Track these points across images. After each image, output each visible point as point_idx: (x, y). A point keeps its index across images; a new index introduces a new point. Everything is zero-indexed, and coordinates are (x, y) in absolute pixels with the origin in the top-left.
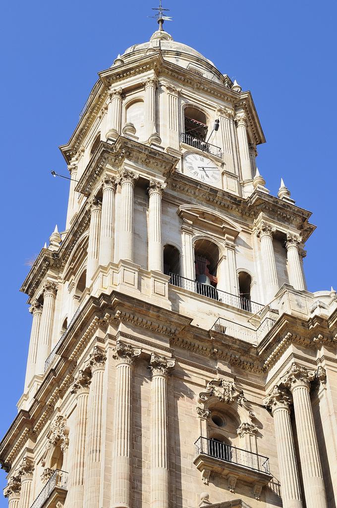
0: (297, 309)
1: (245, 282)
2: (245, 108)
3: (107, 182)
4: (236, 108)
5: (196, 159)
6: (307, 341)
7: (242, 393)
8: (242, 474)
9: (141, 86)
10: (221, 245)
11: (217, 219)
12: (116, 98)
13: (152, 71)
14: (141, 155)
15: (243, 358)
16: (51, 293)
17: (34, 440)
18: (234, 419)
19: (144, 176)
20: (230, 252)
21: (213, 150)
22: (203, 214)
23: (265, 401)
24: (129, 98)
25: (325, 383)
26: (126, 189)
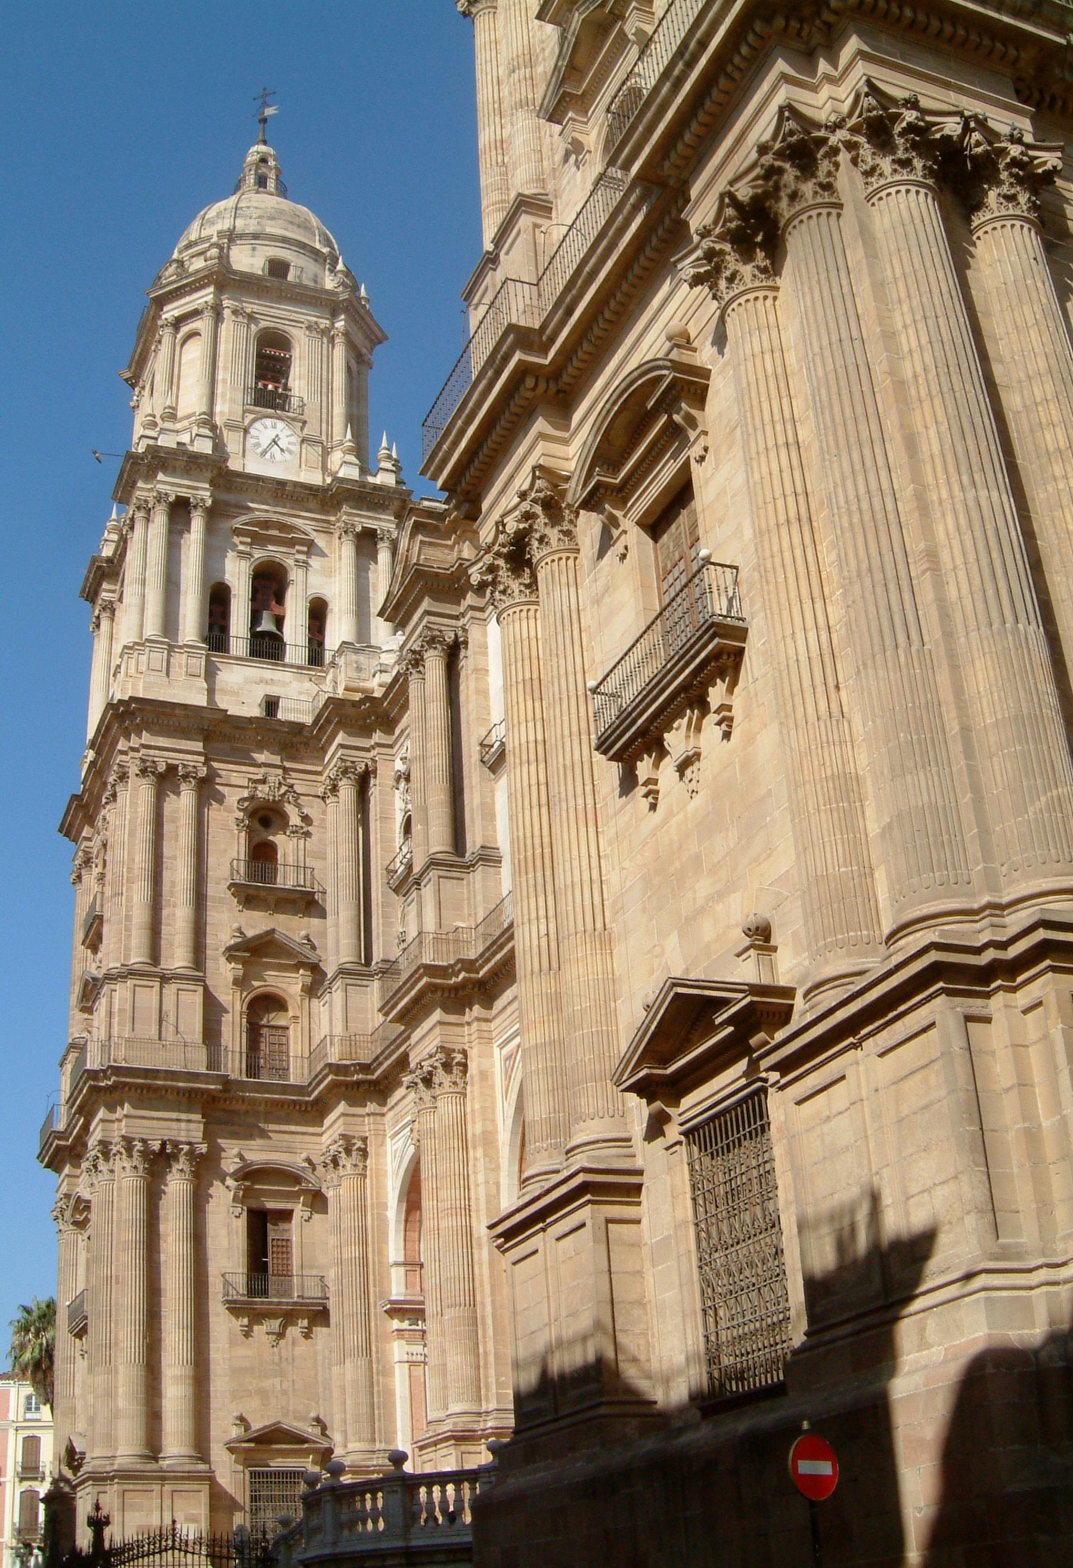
0: (355, 675)
1: (318, 612)
2: (346, 311)
3: (139, 508)
4: (334, 315)
5: (266, 428)
6: (360, 723)
7: (292, 786)
8: (280, 894)
9: (195, 313)
10: (290, 562)
11: (283, 527)
12: (169, 330)
13: (211, 289)
14: (177, 464)
15: (295, 740)
16: (108, 614)
17: (92, 825)
18: (284, 817)
19: (184, 492)
20: (300, 571)
21: (295, 402)
22: (266, 524)
23: (320, 791)
24: (185, 330)
25: (375, 777)
26: (160, 519)
